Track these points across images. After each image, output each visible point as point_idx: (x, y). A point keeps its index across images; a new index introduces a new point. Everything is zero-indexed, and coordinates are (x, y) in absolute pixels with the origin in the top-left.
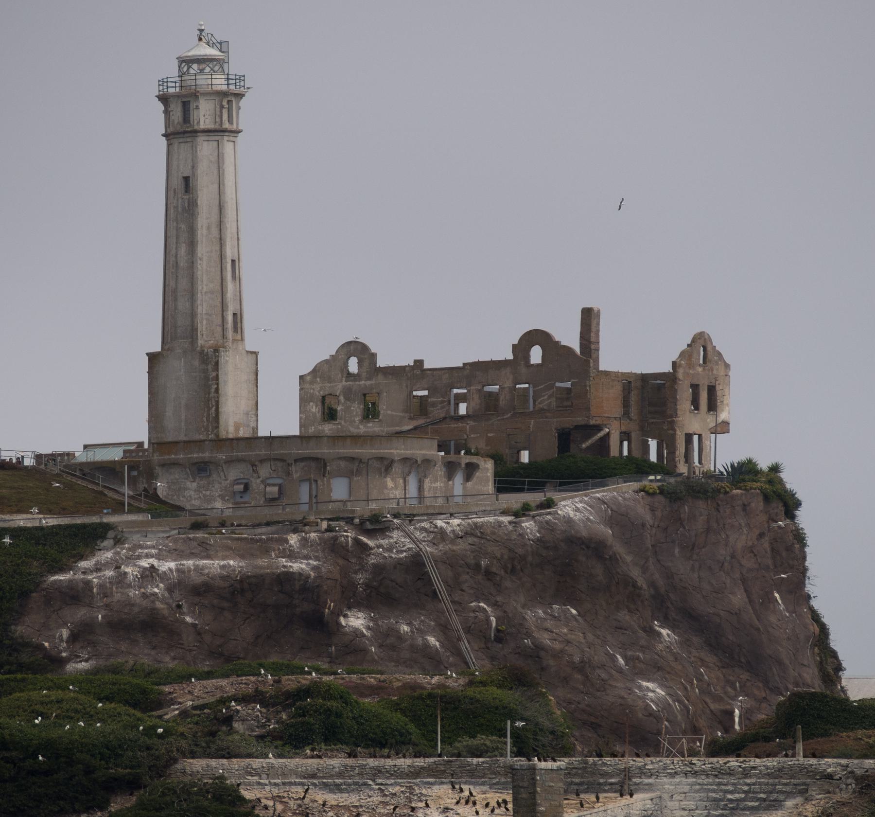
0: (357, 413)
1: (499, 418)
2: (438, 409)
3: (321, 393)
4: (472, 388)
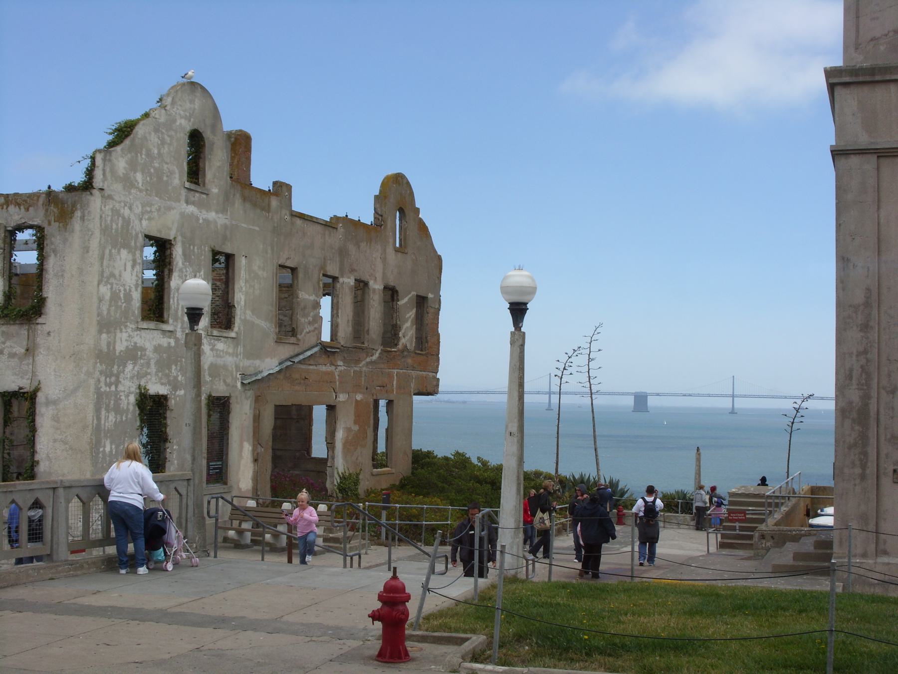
1: (368, 360)
3: (144, 223)
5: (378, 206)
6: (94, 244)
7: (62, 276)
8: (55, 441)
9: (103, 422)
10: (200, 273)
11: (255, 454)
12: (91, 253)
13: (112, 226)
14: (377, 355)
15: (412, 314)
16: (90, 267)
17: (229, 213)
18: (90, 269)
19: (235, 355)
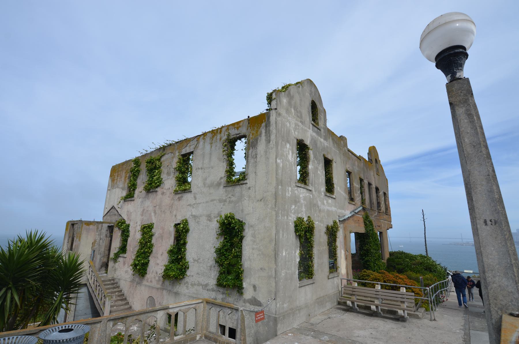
5: (369, 156)
6: (273, 137)
7: (256, 157)
8: (253, 249)
9: (281, 237)
11: (346, 255)
12: (271, 142)
13: (282, 130)
14: (377, 213)
15: (383, 198)
16: (271, 149)
17: (328, 142)
18: (271, 150)
19: (335, 207)
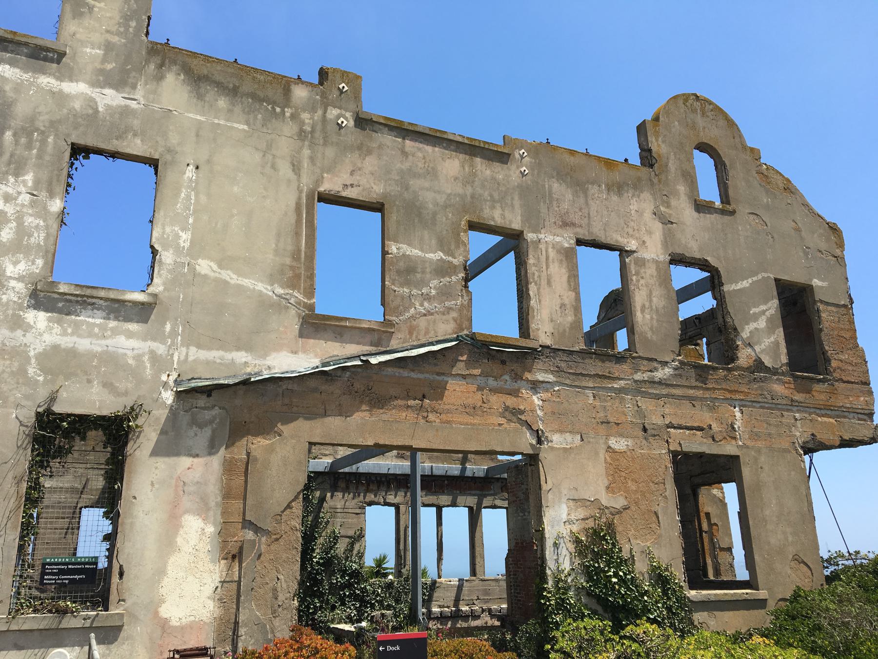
0: (22, 232)
2: (428, 298)
4: (542, 236)
10: (17, 175)
